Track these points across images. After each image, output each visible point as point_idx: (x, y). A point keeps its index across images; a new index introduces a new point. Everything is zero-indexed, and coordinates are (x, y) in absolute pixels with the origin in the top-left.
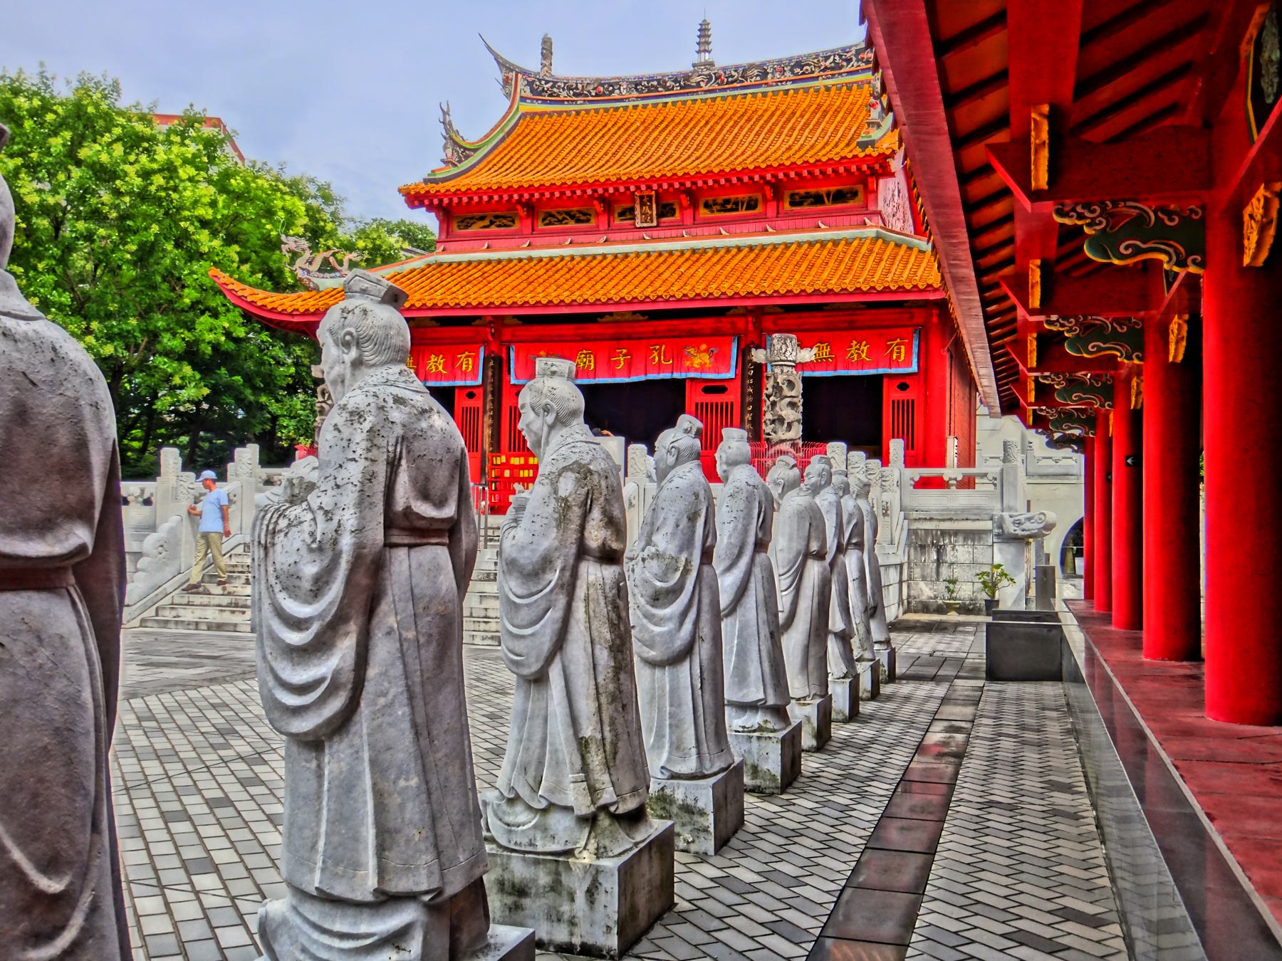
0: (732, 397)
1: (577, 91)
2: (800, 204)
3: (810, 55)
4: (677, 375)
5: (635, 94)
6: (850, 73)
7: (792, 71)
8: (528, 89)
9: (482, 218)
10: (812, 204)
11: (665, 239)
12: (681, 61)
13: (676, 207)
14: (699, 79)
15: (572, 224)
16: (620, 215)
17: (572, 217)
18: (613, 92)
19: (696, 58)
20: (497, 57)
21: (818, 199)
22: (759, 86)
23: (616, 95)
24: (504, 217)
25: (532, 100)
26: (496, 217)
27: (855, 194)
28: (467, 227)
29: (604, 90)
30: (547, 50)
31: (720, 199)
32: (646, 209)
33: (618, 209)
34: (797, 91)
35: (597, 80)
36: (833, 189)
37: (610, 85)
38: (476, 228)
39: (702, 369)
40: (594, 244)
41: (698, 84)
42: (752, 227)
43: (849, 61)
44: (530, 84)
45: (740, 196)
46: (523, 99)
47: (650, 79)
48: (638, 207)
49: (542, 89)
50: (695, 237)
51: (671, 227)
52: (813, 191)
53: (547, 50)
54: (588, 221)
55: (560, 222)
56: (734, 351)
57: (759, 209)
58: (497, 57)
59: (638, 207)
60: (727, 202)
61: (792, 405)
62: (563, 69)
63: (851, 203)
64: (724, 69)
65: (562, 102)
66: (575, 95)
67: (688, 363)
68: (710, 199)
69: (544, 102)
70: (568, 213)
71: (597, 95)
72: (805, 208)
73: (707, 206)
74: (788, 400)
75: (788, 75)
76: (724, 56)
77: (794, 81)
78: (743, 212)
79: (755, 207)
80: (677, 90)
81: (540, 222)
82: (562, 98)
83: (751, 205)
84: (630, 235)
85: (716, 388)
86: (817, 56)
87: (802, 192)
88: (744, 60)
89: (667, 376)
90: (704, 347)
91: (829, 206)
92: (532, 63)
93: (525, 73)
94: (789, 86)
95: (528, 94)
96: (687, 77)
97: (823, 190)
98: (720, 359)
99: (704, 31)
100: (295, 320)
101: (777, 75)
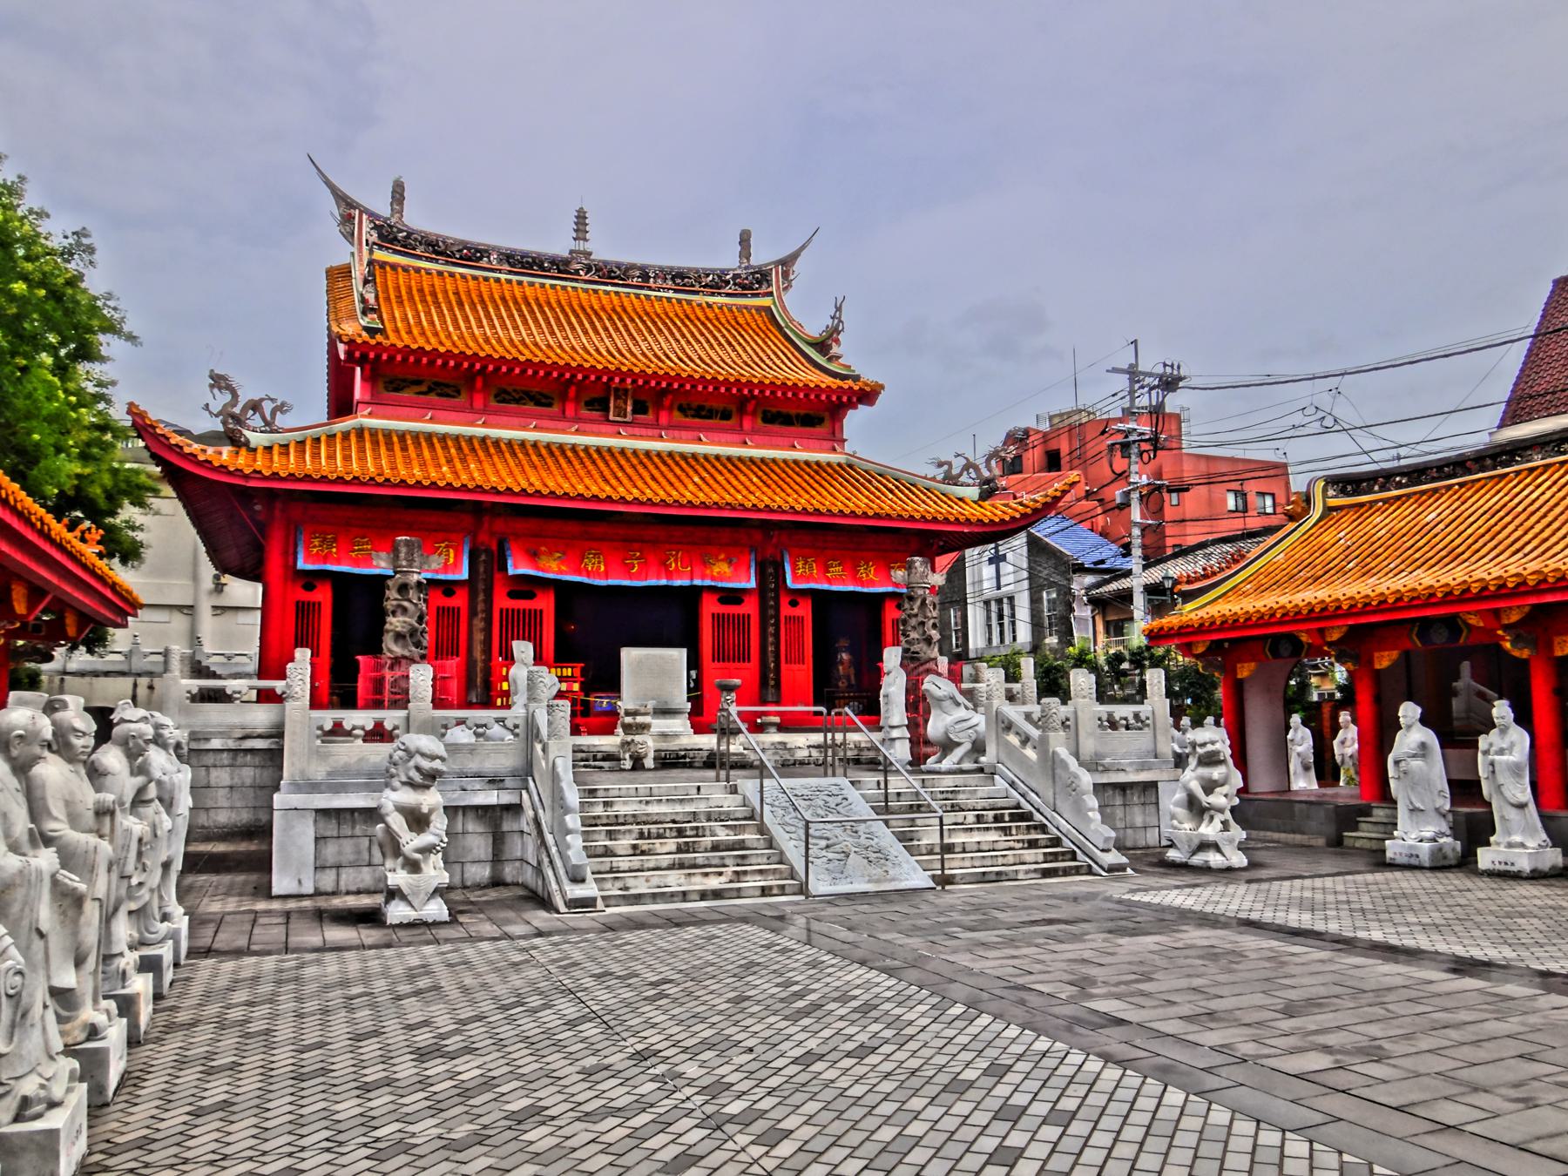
0: (749, 608)
1: (436, 248)
3: (690, 269)
4: (697, 582)
6: (728, 295)
7: (673, 279)
9: (418, 383)
10: (782, 423)
11: (641, 437)
12: (559, 244)
14: (578, 267)
15: (531, 407)
18: (480, 258)
19: (573, 245)
22: (641, 288)
23: (484, 263)
24: (447, 386)
27: (820, 421)
28: (397, 390)
29: (472, 255)
31: (695, 404)
32: (620, 402)
33: (586, 397)
35: (462, 242)
36: (802, 412)
37: (478, 251)
38: (405, 394)
40: (564, 431)
42: (729, 437)
43: (727, 283)
44: (376, 227)
47: (524, 255)
49: (388, 236)
50: (674, 440)
51: (646, 426)
54: (550, 405)
55: (517, 401)
60: (701, 408)
61: (934, 626)
62: (416, 219)
63: (818, 429)
64: (606, 263)
65: (419, 257)
68: (684, 403)
70: (527, 393)
73: (681, 409)
76: (603, 249)
77: (676, 291)
82: (418, 252)
83: (726, 416)
84: (603, 428)
86: (697, 271)
87: (774, 410)
88: (626, 258)
89: (686, 582)
92: (383, 208)
93: (371, 214)
94: (670, 294)
95: (374, 237)
96: (567, 262)
97: (793, 412)
99: (581, 218)
100: (252, 484)
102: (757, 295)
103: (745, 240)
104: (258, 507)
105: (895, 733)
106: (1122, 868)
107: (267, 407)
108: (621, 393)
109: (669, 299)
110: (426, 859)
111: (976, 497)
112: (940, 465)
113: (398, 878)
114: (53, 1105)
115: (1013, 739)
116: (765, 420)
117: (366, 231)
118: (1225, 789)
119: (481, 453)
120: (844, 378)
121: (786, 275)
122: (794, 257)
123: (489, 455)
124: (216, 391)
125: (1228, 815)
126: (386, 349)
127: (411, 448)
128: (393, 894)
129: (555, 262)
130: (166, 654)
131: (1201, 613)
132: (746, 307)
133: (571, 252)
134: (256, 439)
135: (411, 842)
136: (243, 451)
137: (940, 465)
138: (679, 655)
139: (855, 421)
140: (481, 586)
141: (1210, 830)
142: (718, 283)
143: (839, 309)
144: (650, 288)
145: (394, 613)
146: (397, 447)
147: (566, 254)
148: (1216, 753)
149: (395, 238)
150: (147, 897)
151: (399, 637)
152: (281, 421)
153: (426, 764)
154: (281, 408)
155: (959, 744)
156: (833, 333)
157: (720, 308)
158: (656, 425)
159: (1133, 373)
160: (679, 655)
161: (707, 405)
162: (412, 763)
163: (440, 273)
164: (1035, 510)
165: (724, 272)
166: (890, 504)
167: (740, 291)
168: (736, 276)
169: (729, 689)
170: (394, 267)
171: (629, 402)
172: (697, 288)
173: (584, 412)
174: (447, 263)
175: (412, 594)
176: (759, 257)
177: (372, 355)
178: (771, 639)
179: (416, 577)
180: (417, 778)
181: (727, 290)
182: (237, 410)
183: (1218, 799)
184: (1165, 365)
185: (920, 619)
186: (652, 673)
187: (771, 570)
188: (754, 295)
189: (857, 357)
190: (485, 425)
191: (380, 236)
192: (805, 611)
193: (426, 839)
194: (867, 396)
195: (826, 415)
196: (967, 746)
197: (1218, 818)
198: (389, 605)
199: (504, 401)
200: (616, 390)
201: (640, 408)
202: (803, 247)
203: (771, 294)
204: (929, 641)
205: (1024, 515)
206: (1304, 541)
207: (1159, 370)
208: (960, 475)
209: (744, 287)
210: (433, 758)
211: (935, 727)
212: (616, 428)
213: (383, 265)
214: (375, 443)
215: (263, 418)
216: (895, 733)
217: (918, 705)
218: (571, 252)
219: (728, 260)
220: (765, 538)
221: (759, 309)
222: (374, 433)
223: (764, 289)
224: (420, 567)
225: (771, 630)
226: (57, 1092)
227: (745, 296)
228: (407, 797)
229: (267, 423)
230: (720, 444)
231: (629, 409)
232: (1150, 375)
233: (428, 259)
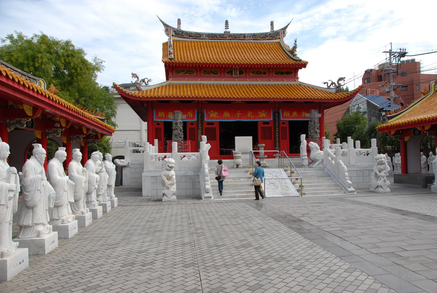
1: (190, 35)
2: (278, 74)
6: (268, 40)
8: (174, 33)
9: (183, 71)
13: (244, 72)
15: (212, 74)
16: (227, 73)
17: (212, 73)
19: (225, 30)
21: (282, 73)
22: (244, 40)
25: (175, 36)
26: (188, 71)
27: (292, 73)
28: (178, 73)
30: (179, 21)
33: (227, 71)
35: (196, 33)
39: (263, 118)
41: (226, 37)
43: (267, 36)
45: (262, 71)
46: (173, 36)
47: (212, 34)
50: (250, 81)
51: (243, 77)
52: (281, 71)
53: (179, 21)
55: (209, 74)
56: (272, 113)
57: (267, 74)
61: (318, 128)
62: (185, 28)
63: (291, 75)
64: (234, 34)
65: (185, 38)
66: (190, 36)
69: (179, 37)
72: (279, 75)
73: (252, 72)
76: (233, 30)
77: (253, 40)
78: (263, 75)
79: (265, 74)
81: (202, 73)
83: (265, 73)
85: (267, 123)
87: (278, 71)
90: (264, 111)
91: (285, 75)
92: (175, 26)
93: (173, 28)
94: (252, 41)
95: (174, 34)
97: (284, 71)
98: (268, 115)
99: (227, 22)
102: (276, 39)
103: (272, 24)
104: (145, 105)
105: (304, 158)
106: (353, 192)
107: (146, 80)
108: (236, 69)
109: (251, 42)
110: (171, 187)
111: (335, 92)
112: (325, 83)
113: (165, 191)
114: (69, 222)
115: (330, 158)
116: (276, 74)
117: (172, 33)
118: (384, 171)
119: (199, 88)
120: (296, 61)
121: (284, 33)
122: (286, 27)
123: (201, 88)
124: (134, 78)
125: (385, 178)
126: (174, 63)
127: (181, 88)
128: (164, 195)
129: (220, 35)
130: (125, 142)
131: (394, 123)
132: (273, 42)
133: (224, 32)
134: (143, 89)
135: (168, 182)
136: (141, 92)
137: (325, 83)
138: (251, 138)
139: (301, 73)
140: (200, 122)
141: (380, 182)
142: (264, 36)
143: (296, 41)
144: (246, 40)
146: (178, 88)
147: (223, 33)
148: (382, 161)
150: (104, 192)
151: (176, 136)
152: (150, 84)
153: (170, 165)
154: (149, 81)
155: (318, 160)
156: (295, 47)
157: (266, 44)
158: (246, 77)
159: (390, 52)
160: (251, 138)
161: (260, 71)
162: (167, 165)
163: (191, 41)
164: (351, 95)
165: (266, 33)
166: (309, 95)
167: (271, 38)
168: (270, 34)
169: (262, 147)
170: (179, 41)
171: (238, 71)
173: (226, 75)
175: (179, 125)
176: (276, 29)
177: (171, 65)
178: (277, 133)
179: (180, 121)
180: (168, 168)
181: (267, 38)
182: (139, 82)
183: (382, 174)
184: (401, 49)
185: (314, 127)
186: (243, 143)
187: (277, 115)
189: (302, 54)
190: (201, 80)
191: (175, 34)
192: (287, 125)
193: (170, 182)
194: (304, 65)
195: (293, 71)
196: (321, 161)
197: (382, 179)
198: (173, 128)
199: (205, 74)
200: (235, 69)
201: (241, 73)
202: (289, 24)
203: (280, 38)
204: (316, 132)
205: (348, 97)
206: (426, 101)
207: (399, 51)
208: (330, 86)
209: (272, 37)
210: (172, 164)
211: (312, 155)
213: (176, 41)
214: (173, 87)
215: (145, 83)
216: (304, 158)
217: (309, 151)
219: (268, 30)
220: (275, 106)
221: (276, 43)
222: (173, 85)
223: (278, 37)
224: (179, 118)
225: (277, 131)
226: (70, 220)
227: (273, 39)
228: (166, 172)
229: (146, 85)
231: (238, 73)
232: (396, 53)
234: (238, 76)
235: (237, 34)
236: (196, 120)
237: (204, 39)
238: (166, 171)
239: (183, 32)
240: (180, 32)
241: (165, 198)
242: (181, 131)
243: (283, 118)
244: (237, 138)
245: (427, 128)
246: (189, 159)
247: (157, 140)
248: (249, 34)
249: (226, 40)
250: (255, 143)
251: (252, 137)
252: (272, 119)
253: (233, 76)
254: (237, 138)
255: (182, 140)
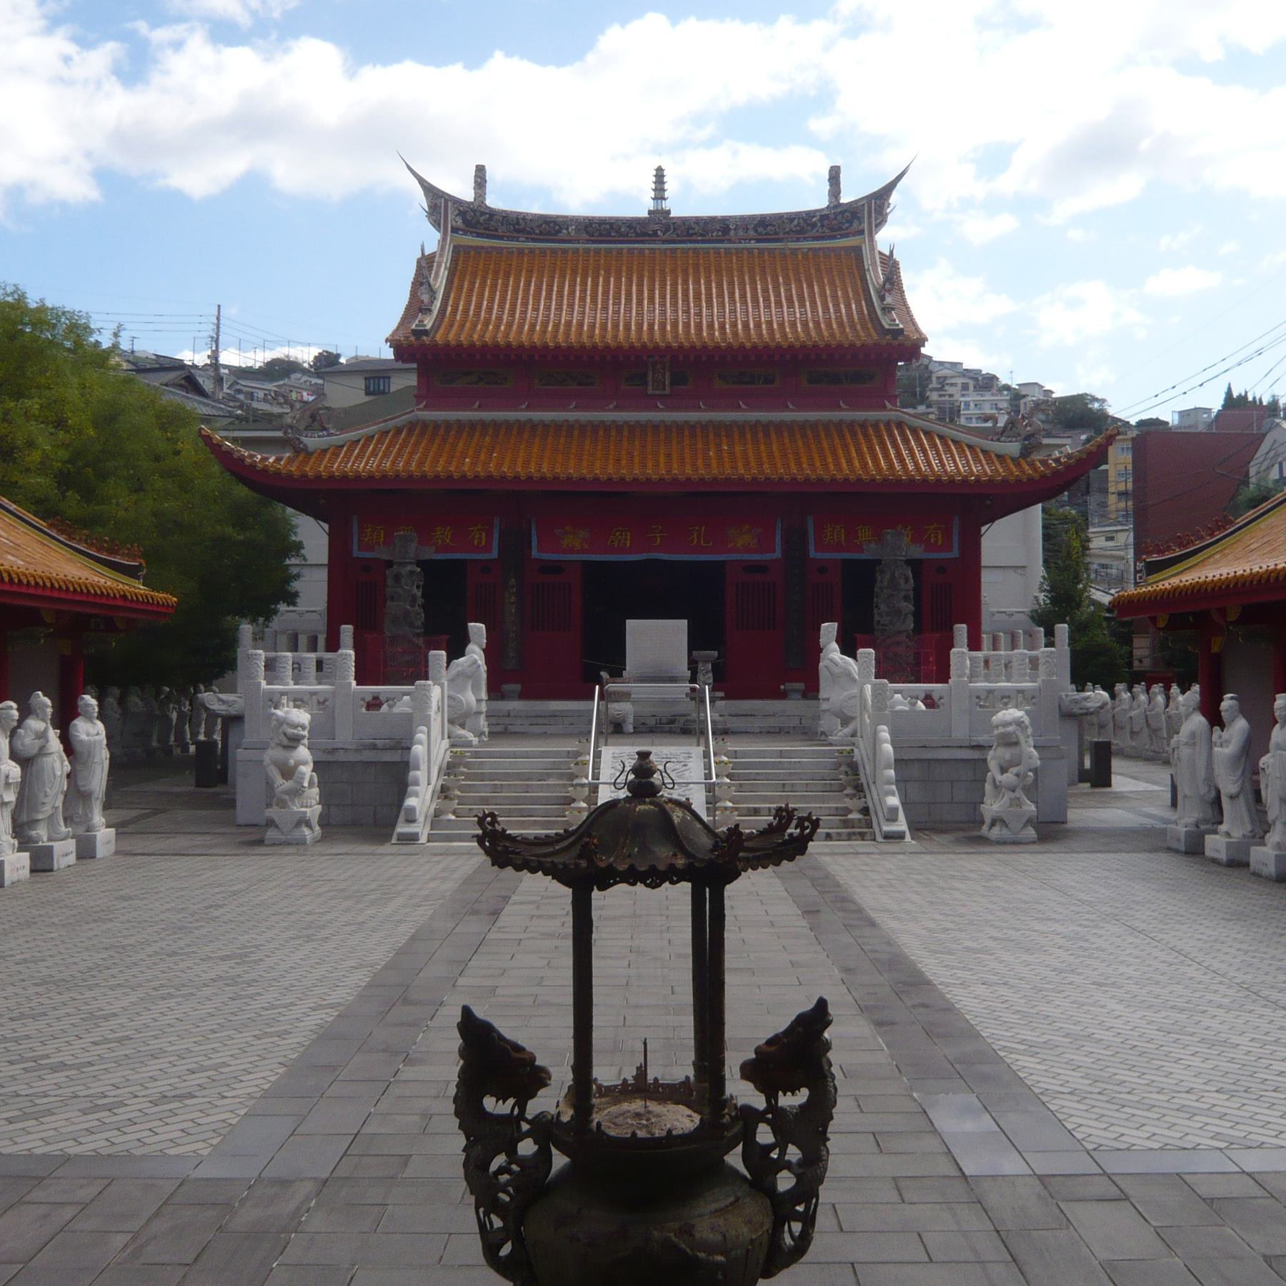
5: (585, 236)
8: (460, 221)
14: (656, 227)
18: (559, 231)
20: (422, 182)
23: (560, 236)
25: (465, 233)
34: (761, 251)
39: (747, 550)
41: (655, 233)
43: (814, 225)
46: (455, 230)
48: (650, 373)
58: (422, 182)
59: (650, 373)
61: (906, 598)
65: (501, 238)
67: (731, 545)
69: (479, 235)
71: (541, 233)
74: (903, 594)
75: (752, 233)
77: (758, 241)
79: (772, 381)
80: (632, 236)
82: (500, 232)
94: (753, 244)
101: (741, 233)
102: (847, 235)
106: (899, 836)
109: (750, 251)
110: (292, 800)
117: (453, 219)
118: (1014, 770)
125: (1019, 793)
132: (834, 249)
135: (282, 784)
144: (730, 241)
145: (392, 599)
147: (646, 215)
149: (478, 222)
172: (781, 235)
174: (527, 240)
176: (845, 199)
181: (814, 233)
186: (656, 641)
188: (843, 236)
193: (288, 785)
212: (649, 403)
218: (650, 212)
219: (817, 200)
227: (834, 237)
230: (760, 409)
233: (510, 238)
234: (668, 391)
235: (698, 220)
236: (494, 554)
237: (569, 241)
238: (280, 748)
239: (492, 214)
240: (483, 214)
241: (271, 834)
242: (413, 600)
243: (817, 550)
244: (631, 624)
245: (1232, 617)
246: (391, 707)
247: (350, 627)
248: (742, 218)
249: (654, 242)
250: (695, 642)
251: (686, 621)
252: (778, 554)
253: (650, 391)
254: (631, 624)
255: (418, 635)
